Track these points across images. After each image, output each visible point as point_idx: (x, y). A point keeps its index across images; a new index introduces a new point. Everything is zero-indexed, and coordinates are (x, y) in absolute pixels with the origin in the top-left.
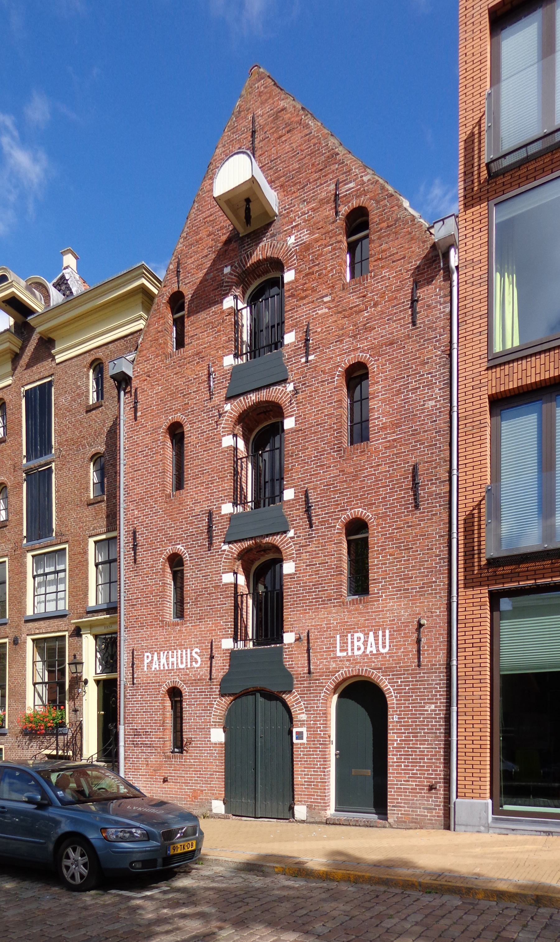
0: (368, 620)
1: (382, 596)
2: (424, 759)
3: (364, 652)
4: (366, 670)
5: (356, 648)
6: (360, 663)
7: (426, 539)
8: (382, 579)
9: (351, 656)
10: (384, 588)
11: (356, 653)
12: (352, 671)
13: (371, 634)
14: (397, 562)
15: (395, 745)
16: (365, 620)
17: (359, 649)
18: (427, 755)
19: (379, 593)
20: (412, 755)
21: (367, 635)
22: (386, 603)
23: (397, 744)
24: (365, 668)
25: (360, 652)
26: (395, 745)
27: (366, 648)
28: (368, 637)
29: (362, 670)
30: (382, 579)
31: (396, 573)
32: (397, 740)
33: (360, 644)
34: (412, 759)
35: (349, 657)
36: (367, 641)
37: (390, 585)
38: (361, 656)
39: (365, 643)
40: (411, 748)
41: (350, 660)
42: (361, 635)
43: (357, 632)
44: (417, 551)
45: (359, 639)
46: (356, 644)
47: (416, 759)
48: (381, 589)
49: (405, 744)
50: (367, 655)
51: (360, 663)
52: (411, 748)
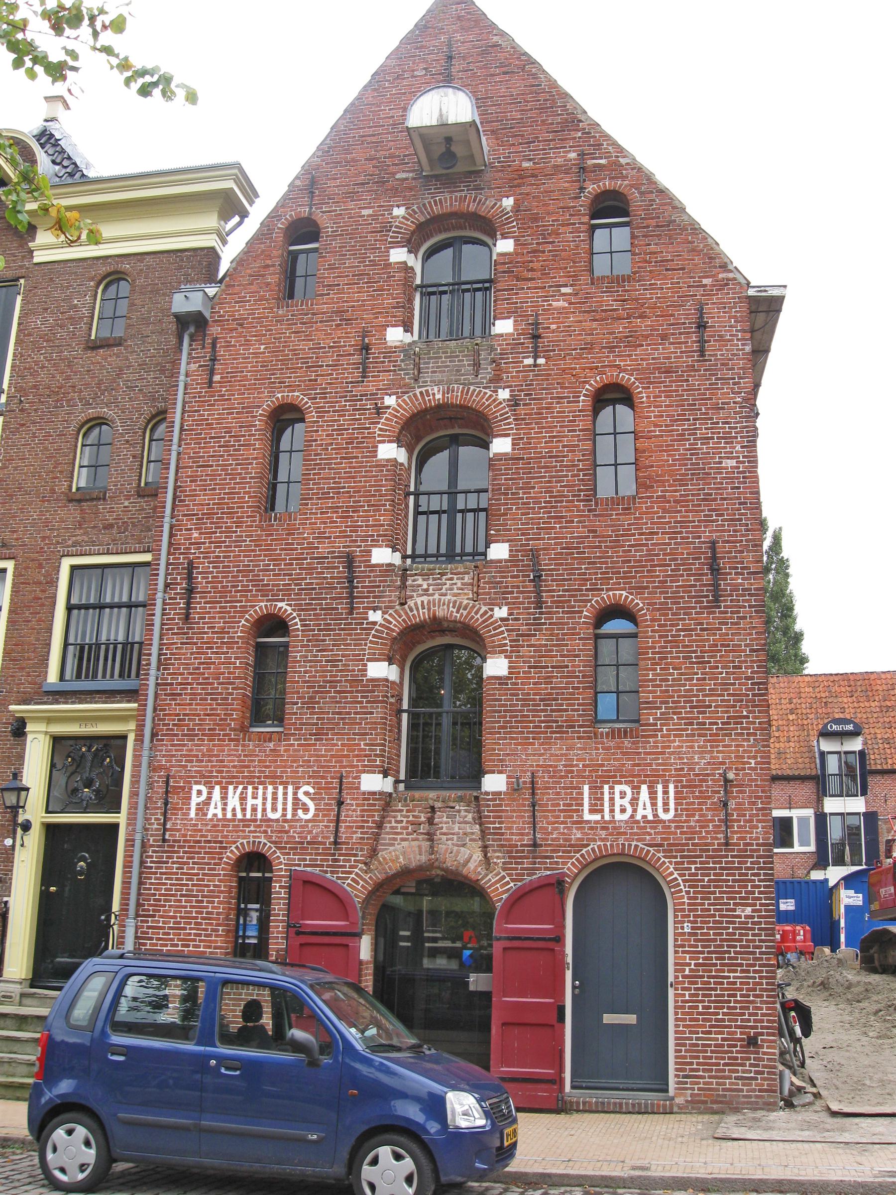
0: (638, 765)
1: (661, 730)
2: (735, 996)
3: (632, 816)
4: (636, 846)
5: (617, 809)
6: (625, 833)
7: (730, 651)
8: (661, 703)
9: (610, 822)
10: (665, 718)
11: (619, 816)
12: (611, 845)
13: (644, 788)
14: (686, 680)
15: (687, 972)
16: (634, 765)
17: (623, 811)
18: (741, 990)
19: (656, 725)
20: (715, 989)
21: (636, 789)
22: (669, 741)
23: (691, 970)
24: (634, 843)
25: (626, 817)
26: (687, 972)
27: (635, 811)
28: (638, 793)
29: (630, 845)
30: (661, 703)
31: (684, 696)
32: (689, 965)
33: (626, 802)
34: (716, 996)
35: (605, 822)
36: (638, 799)
37: (674, 713)
38: (626, 822)
39: (634, 801)
40: (714, 977)
41: (606, 828)
42: (628, 789)
43: (620, 783)
44: (717, 667)
45: (623, 795)
46: (618, 802)
47: (723, 995)
48: (660, 719)
49: (703, 971)
50: (638, 822)
51: (625, 833)
52: (714, 977)
